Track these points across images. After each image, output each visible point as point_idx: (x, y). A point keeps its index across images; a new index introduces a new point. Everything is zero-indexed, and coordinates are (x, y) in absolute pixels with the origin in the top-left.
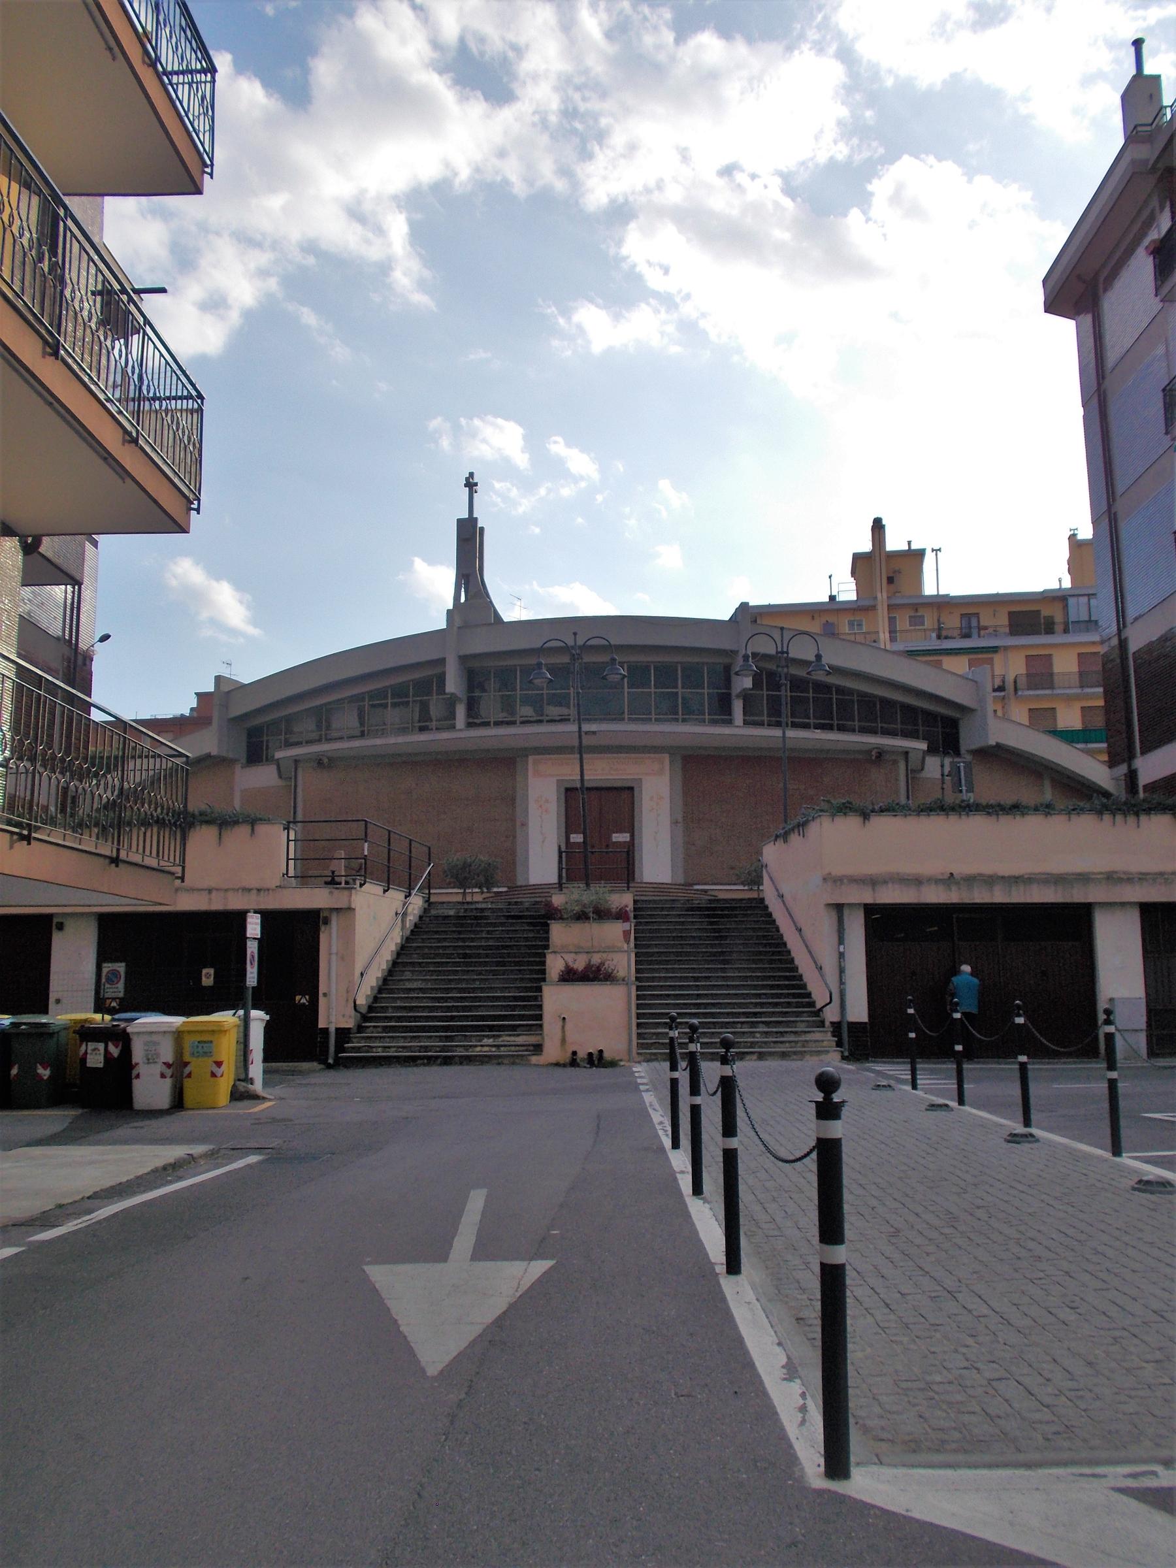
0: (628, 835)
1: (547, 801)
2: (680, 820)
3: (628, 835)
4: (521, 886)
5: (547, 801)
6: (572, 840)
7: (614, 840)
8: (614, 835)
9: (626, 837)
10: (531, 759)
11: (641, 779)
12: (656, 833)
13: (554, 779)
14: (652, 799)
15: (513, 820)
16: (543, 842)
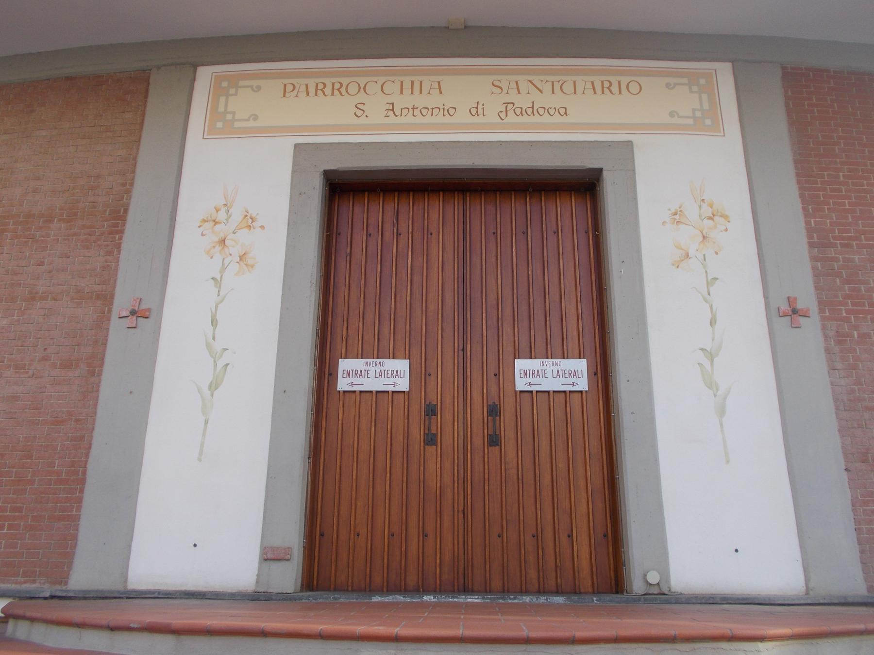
0: (581, 365)
1: (249, 221)
2: (807, 299)
3: (581, 365)
4: (86, 596)
5: (249, 221)
6: (343, 384)
7: (521, 384)
8: (521, 364)
9: (575, 374)
10: (205, 75)
11: (629, 144)
12: (711, 356)
13: (285, 146)
14: (677, 217)
15: (107, 298)
16: (214, 386)
